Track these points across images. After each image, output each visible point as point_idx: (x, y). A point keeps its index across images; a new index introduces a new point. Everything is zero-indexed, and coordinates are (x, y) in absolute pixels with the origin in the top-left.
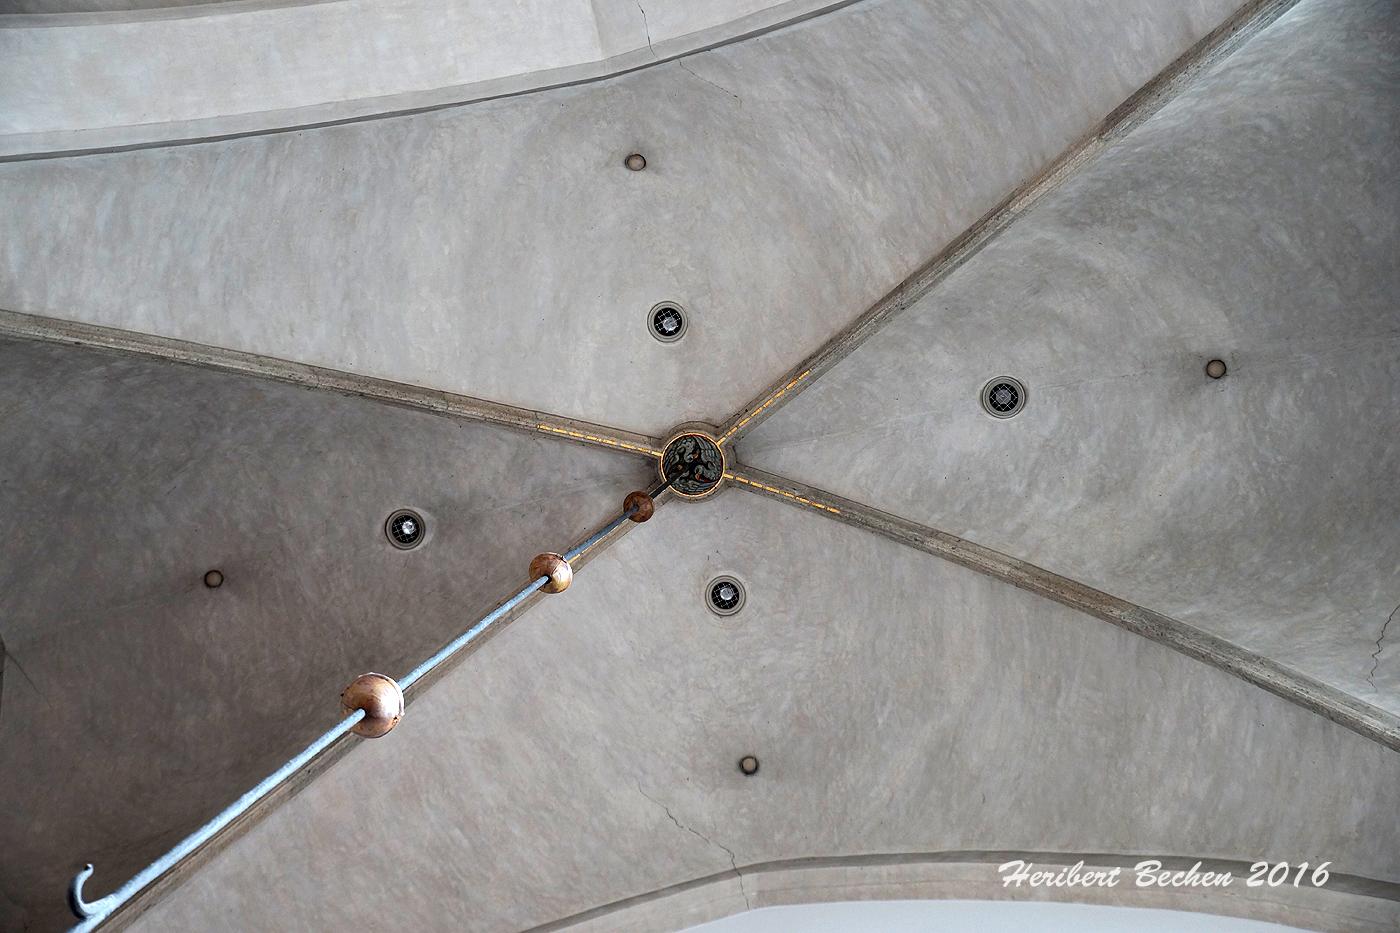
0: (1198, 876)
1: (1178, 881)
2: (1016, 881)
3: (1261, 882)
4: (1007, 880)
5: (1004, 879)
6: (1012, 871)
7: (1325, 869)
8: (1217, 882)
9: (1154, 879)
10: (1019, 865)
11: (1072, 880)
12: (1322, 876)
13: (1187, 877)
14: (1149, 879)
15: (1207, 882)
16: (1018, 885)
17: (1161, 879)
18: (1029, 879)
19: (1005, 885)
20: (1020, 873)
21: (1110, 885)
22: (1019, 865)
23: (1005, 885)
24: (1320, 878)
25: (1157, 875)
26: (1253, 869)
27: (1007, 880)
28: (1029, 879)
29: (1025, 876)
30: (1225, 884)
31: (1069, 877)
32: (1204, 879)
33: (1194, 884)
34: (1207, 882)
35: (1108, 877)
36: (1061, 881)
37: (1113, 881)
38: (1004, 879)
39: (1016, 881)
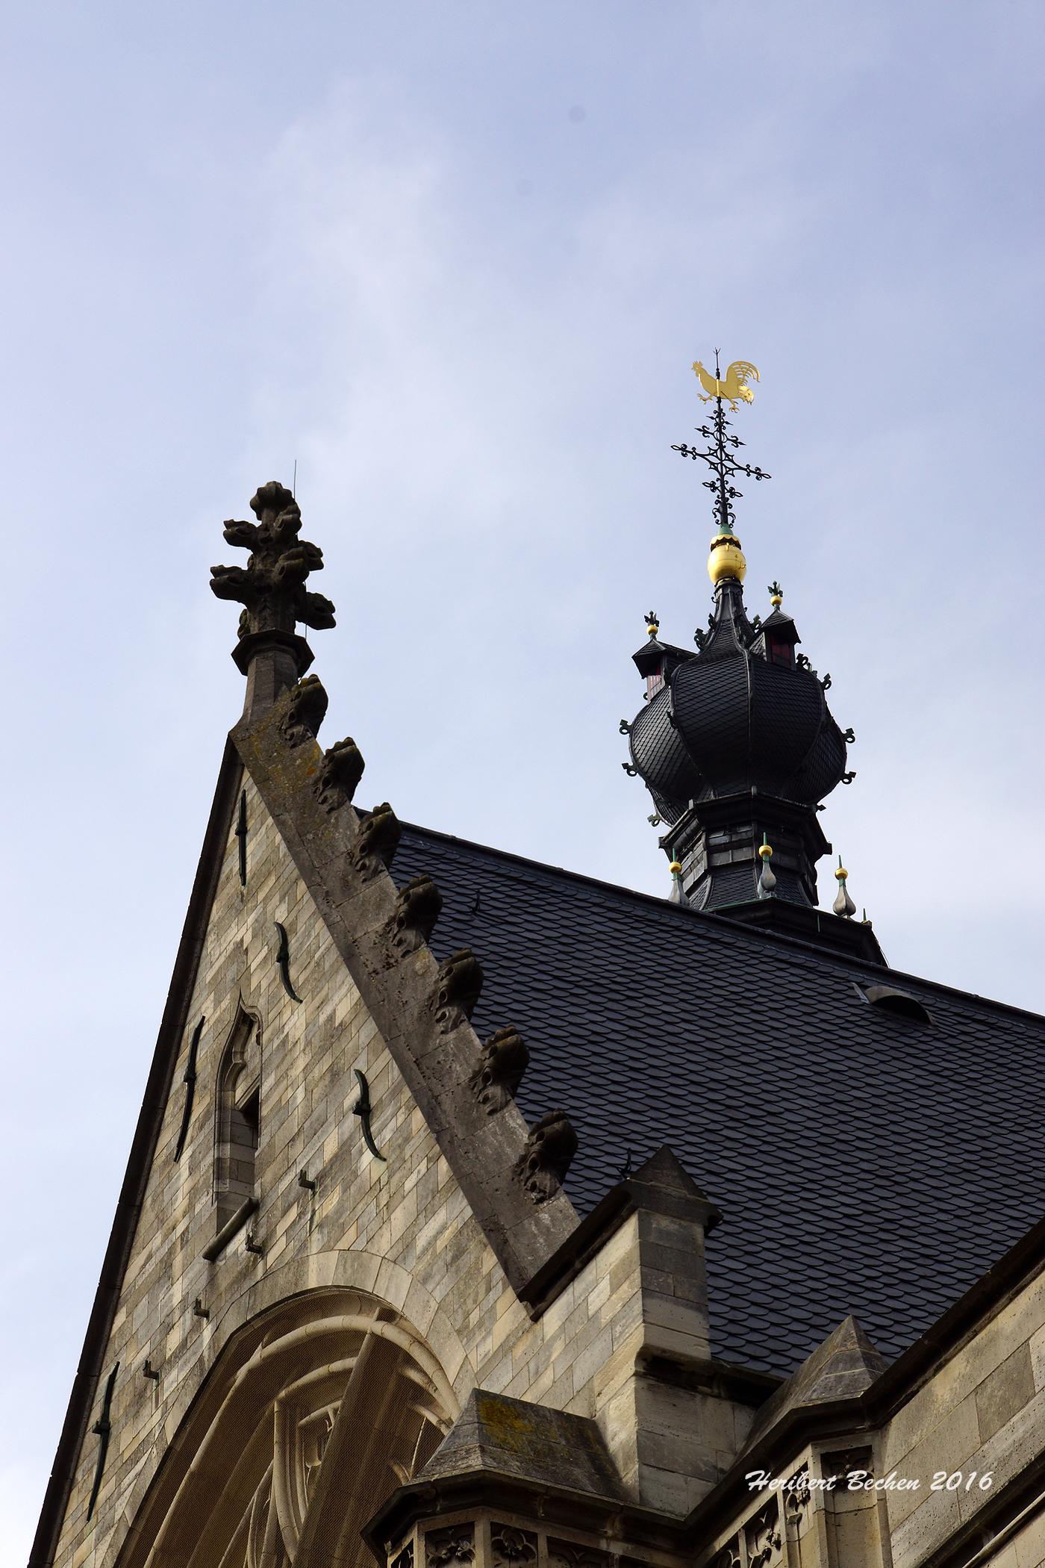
0: (894, 1482)
1: (879, 1485)
2: (759, 1486)
3: (941, 1487)
4: (752, 1485)
5: (750, 1484)
6: (754, 1478)
7: (989, 1477)
8: (908, 1487)
9: (862, 1484)
10: (760, 1474)
11: (800, 1485)
12: (987, 1482)
13: (887, 1482)
14: (859, 1484)
15: (901, 1486)
16: (760, 1488)
17: (866, 1484)
18: (768, 1484)
19: (750, 1489)
20: (762, 1479)
21: (829, 1489)
22: (760, 1474)
23: (750, 1489)
24: (985, 1484)
25: (864, 1481)
26: (935, 1477)
27: (752, 1485)
28: (768, 1484)
29: (765, 1482)
30: (914, 1488)
31: (799, 1482)
32: (899, 1484)
33: (891, 1488)
34: (901, 1486)
35: (828, 1483)
36: (793, 1485)
37: (831, 1486)
38: (750, 1484)
39: (759, 1486)
